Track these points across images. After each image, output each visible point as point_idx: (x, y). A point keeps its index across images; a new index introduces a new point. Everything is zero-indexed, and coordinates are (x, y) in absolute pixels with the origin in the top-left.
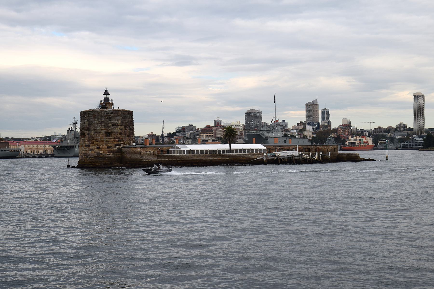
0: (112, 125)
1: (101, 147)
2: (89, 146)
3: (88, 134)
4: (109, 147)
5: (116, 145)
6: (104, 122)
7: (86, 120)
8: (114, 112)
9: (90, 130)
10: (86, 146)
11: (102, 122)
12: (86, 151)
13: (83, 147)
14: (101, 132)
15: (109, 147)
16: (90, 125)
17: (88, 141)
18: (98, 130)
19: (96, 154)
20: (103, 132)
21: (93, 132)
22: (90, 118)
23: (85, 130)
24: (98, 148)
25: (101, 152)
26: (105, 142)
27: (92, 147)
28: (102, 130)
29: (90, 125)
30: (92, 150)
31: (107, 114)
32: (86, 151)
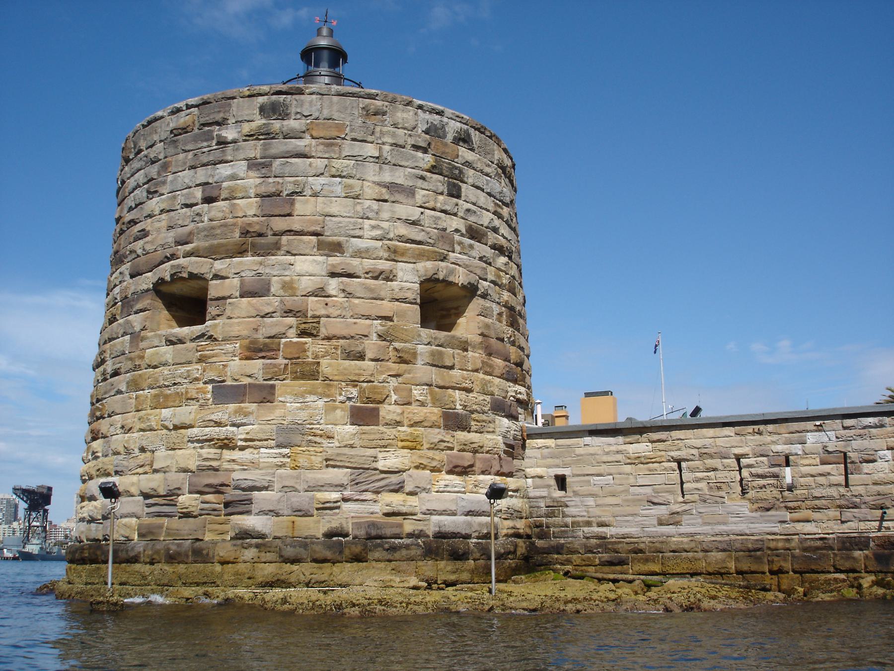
0: (475, 233)
1: (389, 411)
2: (265, 394)
3: (255, 290)
4: (455, 421)
5: (500, 408)
6: (410, 192)
7: (224, 170)
8: (475, 136)
9: (274, 249)
10: (225, 392)
11: (392, 187)
12: (226, 444)
13: (186, 413)
14: (389, 277)
15: (455, 421)
16: (277, 201)
17: (255, 350)
18: (359, 254)
19: (340, 475)
20: (408, 277)
21: (307, 267)
22: (279, 146)
23: (213, 253)
24: (364, 415)
25: (390, 460)
26: (421, 370)
27: (292, 404)
28: (394, 255)
29: (277, 201)
30: (289, 437)
31: (434, 131)
32: (226, 444)
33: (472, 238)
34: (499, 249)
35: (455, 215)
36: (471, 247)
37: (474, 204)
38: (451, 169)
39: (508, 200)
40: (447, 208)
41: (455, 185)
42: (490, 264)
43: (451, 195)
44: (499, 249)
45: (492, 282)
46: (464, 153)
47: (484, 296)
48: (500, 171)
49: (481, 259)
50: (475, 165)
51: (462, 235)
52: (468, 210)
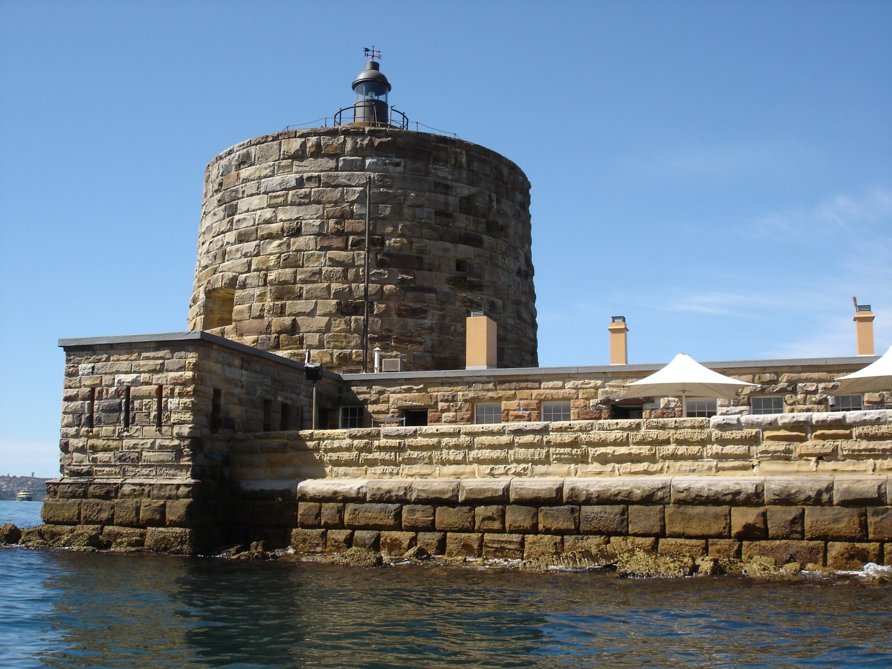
0: (242, 238)
33: (241, 242)
34: (271, 237)
35: (229, 230)
36: (237, 250)
37: (248, 211)
38: (230, 195)
39: (293, 183)
40: (223, 229)
41: (231, 206)
42: (258, 255)
43: (229, 216)
44: (271, 237)
45: (254, 271)
46: (245, 172)
47: (244, 286)
48: (284, 163)
49: (245, 255)
50: (252, 178)
51: (232, 244)
52: (239, 221)
